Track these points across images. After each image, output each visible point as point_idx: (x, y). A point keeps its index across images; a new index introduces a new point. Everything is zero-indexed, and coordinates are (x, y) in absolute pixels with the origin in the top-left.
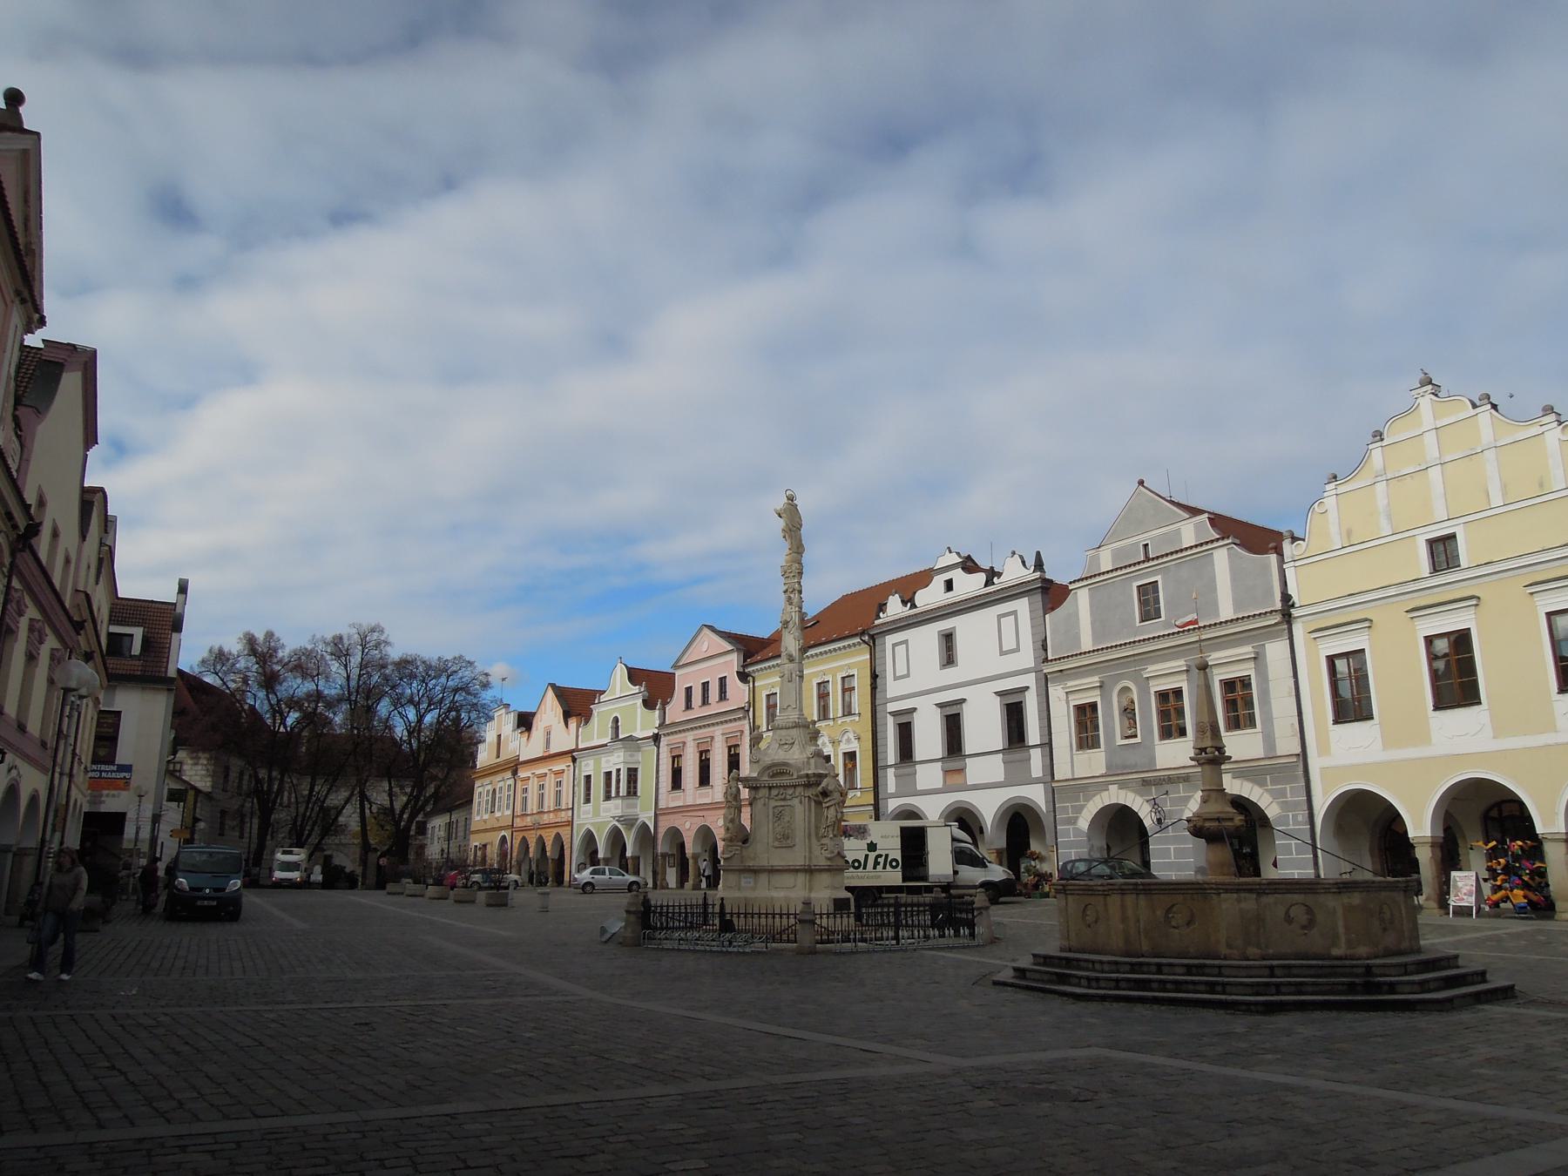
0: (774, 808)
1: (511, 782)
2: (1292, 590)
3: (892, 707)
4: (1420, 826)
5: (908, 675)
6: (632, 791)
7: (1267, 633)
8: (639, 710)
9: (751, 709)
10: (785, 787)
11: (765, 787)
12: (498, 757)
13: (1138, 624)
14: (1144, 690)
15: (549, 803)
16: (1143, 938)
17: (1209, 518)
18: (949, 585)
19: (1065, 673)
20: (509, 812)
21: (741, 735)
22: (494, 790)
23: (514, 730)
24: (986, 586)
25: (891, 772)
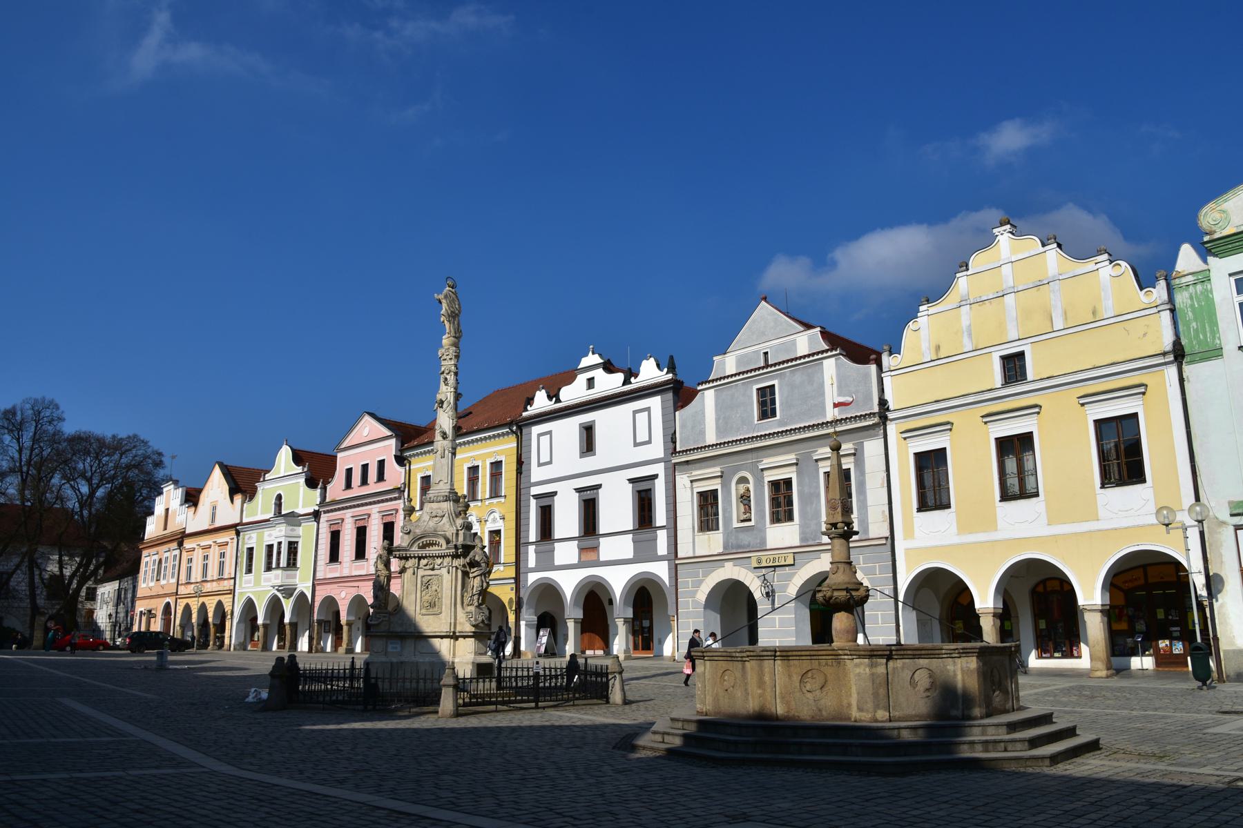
0: (423, 577)
1: (177, 552)
2: (888, 396)
3: (535, 490)
4: (985, 600)
5: (550, 462)
6: (292, 563)
8: (302, 489)
9: (407, 490)
10: (433, 557)
11: (415, 557)
12: (165, 529)
13: (756, 422)
14: (759, 481)
15: (213, 573)
16: (778, 701)
17: (820, 331)
18: (591, 383)
20: (174, 581)
21: (396, 514)
22: (160, 561)
23: (181, 505)
24: (624, 384)
25: (532, 549)
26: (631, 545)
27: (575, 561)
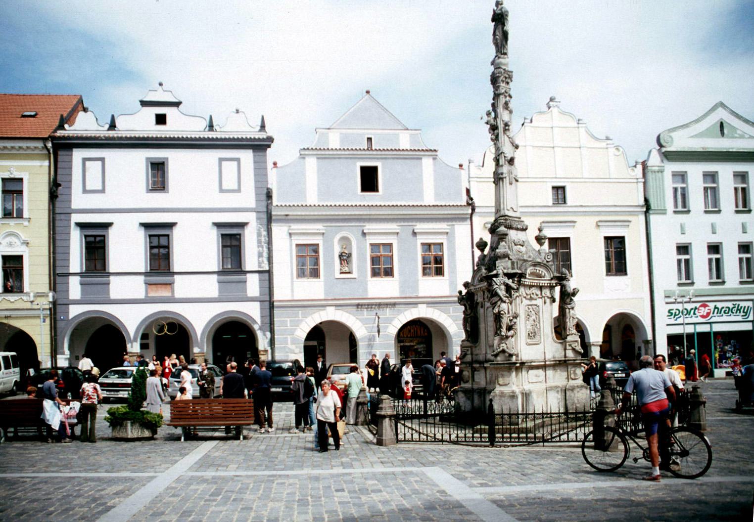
3: (76, 218)
5: (103, 191)
7: (460, 218)
18: (161, 119)
19: (289, 217)
26: (216, 286)
27: (142, 296)
